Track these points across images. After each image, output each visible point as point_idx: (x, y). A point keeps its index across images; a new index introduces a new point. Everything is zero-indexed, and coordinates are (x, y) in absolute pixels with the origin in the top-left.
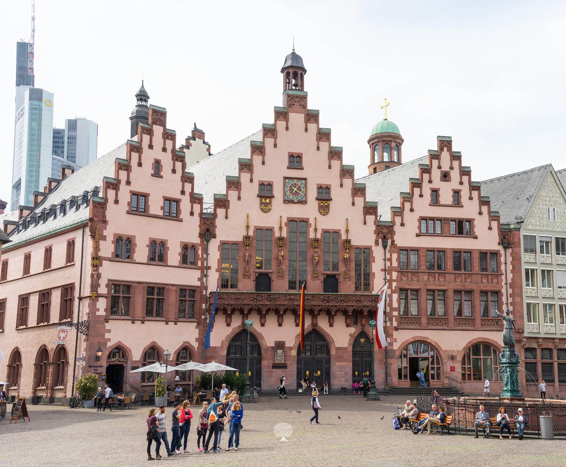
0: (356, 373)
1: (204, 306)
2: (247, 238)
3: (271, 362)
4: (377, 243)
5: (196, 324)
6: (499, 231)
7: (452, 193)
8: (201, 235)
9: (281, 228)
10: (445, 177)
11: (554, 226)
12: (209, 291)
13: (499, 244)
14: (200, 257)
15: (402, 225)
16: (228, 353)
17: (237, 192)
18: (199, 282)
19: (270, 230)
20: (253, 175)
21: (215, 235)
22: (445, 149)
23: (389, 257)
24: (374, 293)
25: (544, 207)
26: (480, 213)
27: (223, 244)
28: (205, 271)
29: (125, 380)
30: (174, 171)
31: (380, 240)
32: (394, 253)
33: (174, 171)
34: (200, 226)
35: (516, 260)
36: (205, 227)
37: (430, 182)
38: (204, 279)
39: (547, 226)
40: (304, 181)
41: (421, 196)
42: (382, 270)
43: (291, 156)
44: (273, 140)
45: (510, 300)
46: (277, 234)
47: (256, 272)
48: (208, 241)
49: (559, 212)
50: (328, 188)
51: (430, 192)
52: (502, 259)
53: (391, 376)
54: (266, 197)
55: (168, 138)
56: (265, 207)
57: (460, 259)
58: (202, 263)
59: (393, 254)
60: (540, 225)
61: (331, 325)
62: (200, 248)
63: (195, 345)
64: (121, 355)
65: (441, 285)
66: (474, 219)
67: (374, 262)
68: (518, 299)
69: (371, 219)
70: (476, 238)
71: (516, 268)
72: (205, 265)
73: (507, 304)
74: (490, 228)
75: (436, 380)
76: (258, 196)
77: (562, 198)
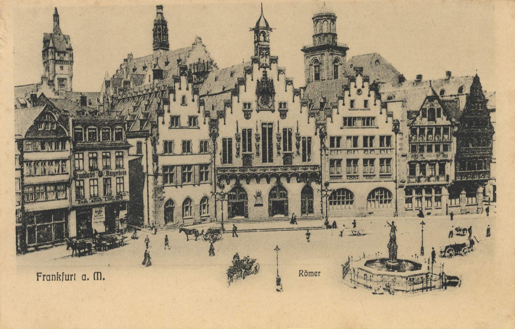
4: (316, 134)
8: (210, 135)
15: (332, 122)
19: (250, 131)
22: (359, 75)
26: (381, 113)
30: (193, 101)
33: (193, 101)
37: (350, 96)
41: (344, 104)
46: (254, 132)
50: (285, 104)
51: (349, 102)
57: (368, 140)
61: (288, 182)
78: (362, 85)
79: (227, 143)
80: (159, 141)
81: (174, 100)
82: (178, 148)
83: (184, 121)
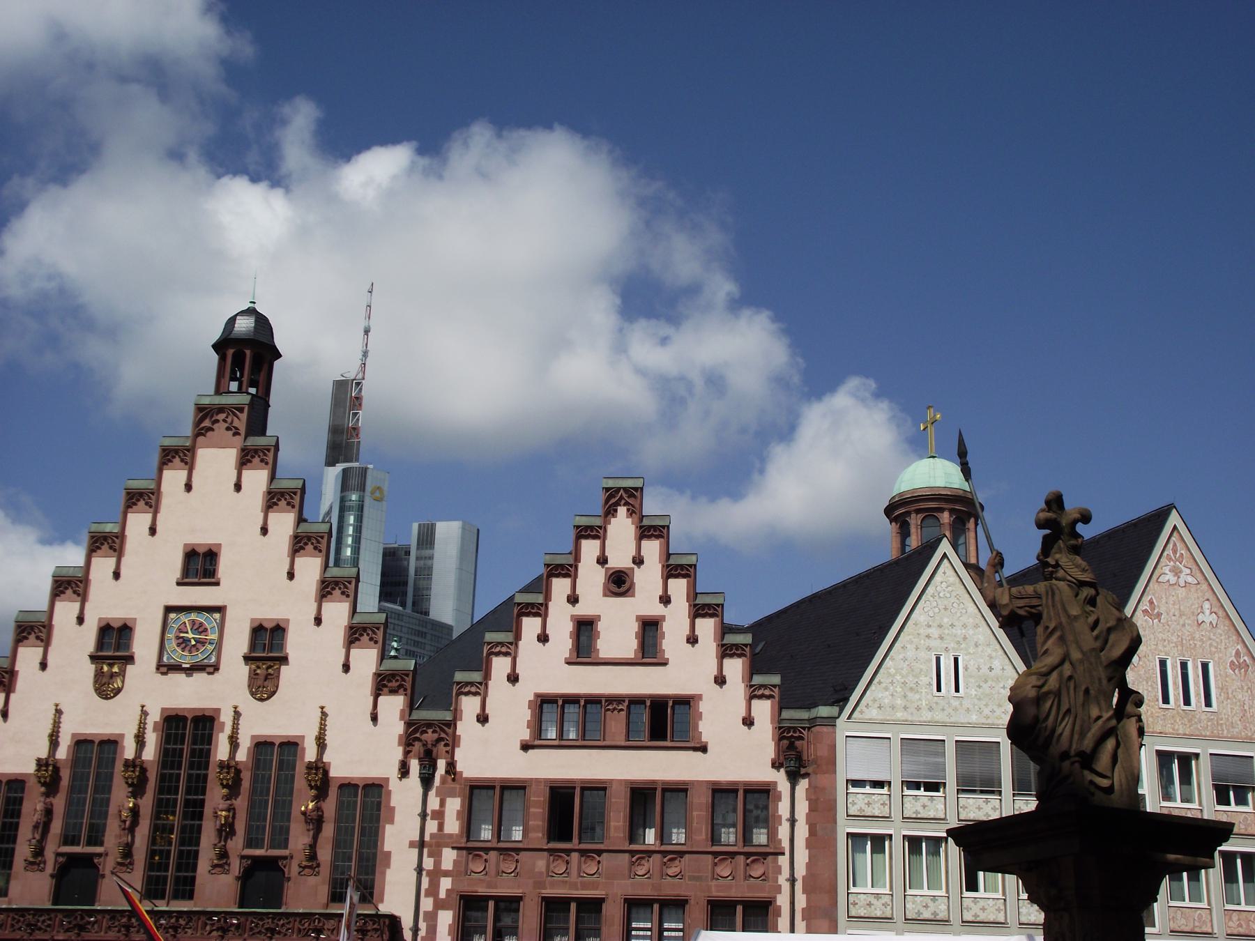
4: (404, 771)
7: (635, 627)
9: (140, 740)
10: (619, 583)
11: (955, 709)
13: (776, 765)
15: (483, 719)
19: (111, 744)
20: (87, 605)
23: (437, 807)
24: (384, 908)
25: (923, 654)
26: (720, 680)
31: (414, 765)
32: (454, 796)
35: (823, 809)
37: (573, 599)
39: (931, 709)
40: (217, 616)
41: (543, 638)
42: (412, 844)
43: (191, 555)
44: (148, 518)
46: (129, 752)
47: (58, 855)
49: (972, 668)
50: (279, 631)
51: (569, 627)
54: (112, 660)
56: (106, 687)
59: (449, 801)
60: (905, 708)
65: (585, 886)
66: (700, 697)
67: (392, 821)
69: (393, 705)
70: (703, 749)
71: (820, 832)
74: (748, 722)
78: (632, 552)
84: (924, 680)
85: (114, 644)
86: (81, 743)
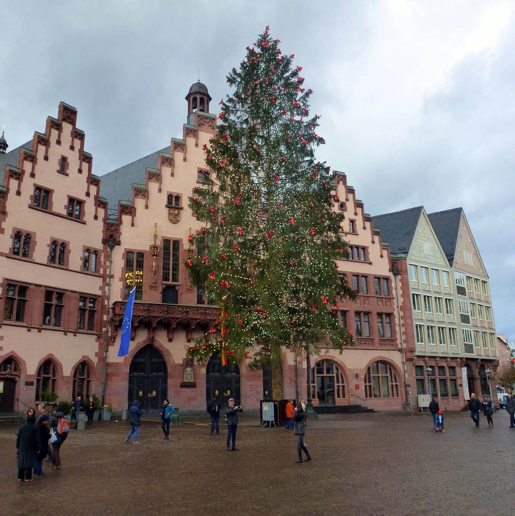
0: (267, 392)
1: (105, 318)
2: (155, 247)
3: (179, 381)
5: (96, 337)
6: (389, 259)
8: (105, 242)
12: (112, 301)
13: (390, 271)
14: (103, 264)
16: (131, 371)
17: (144, 201)
18: (101, 291)
21: (120, 241)
22: (341, 182)
25: (421, 241)
26: (373, 242)
27: (129, 252)
28: (108, 279)
29: (16, 397)
30: (80, 171)
33: (80, 171)
34: (103, 231)
35: (405, 285)
36: (109, 233)
38: (107, 288)
45: (402, 322)
46: (186, 245)
48: (112, 248)
52: (393, 285)
53: (301, 395)
55: (76, 137)
56: (174, 219)
58: (105, 271)
62: (103, 254)
63: (95, 360)
64: (13, 366)
65: (343, 306)
68: (409, 321)
70: (371, 264)
72: (108, 273)
73: (399, 325)
74: (382, 256)
75: (341, 398)
76: (167, 206)
77: (432, 236)
79: (135, 260)
80: (4, 225)
81: (46, 158)
82: (41, 252)
83: (59, 204)
84: (422, 249)
85: (173, 202)
86: (166, 241)
